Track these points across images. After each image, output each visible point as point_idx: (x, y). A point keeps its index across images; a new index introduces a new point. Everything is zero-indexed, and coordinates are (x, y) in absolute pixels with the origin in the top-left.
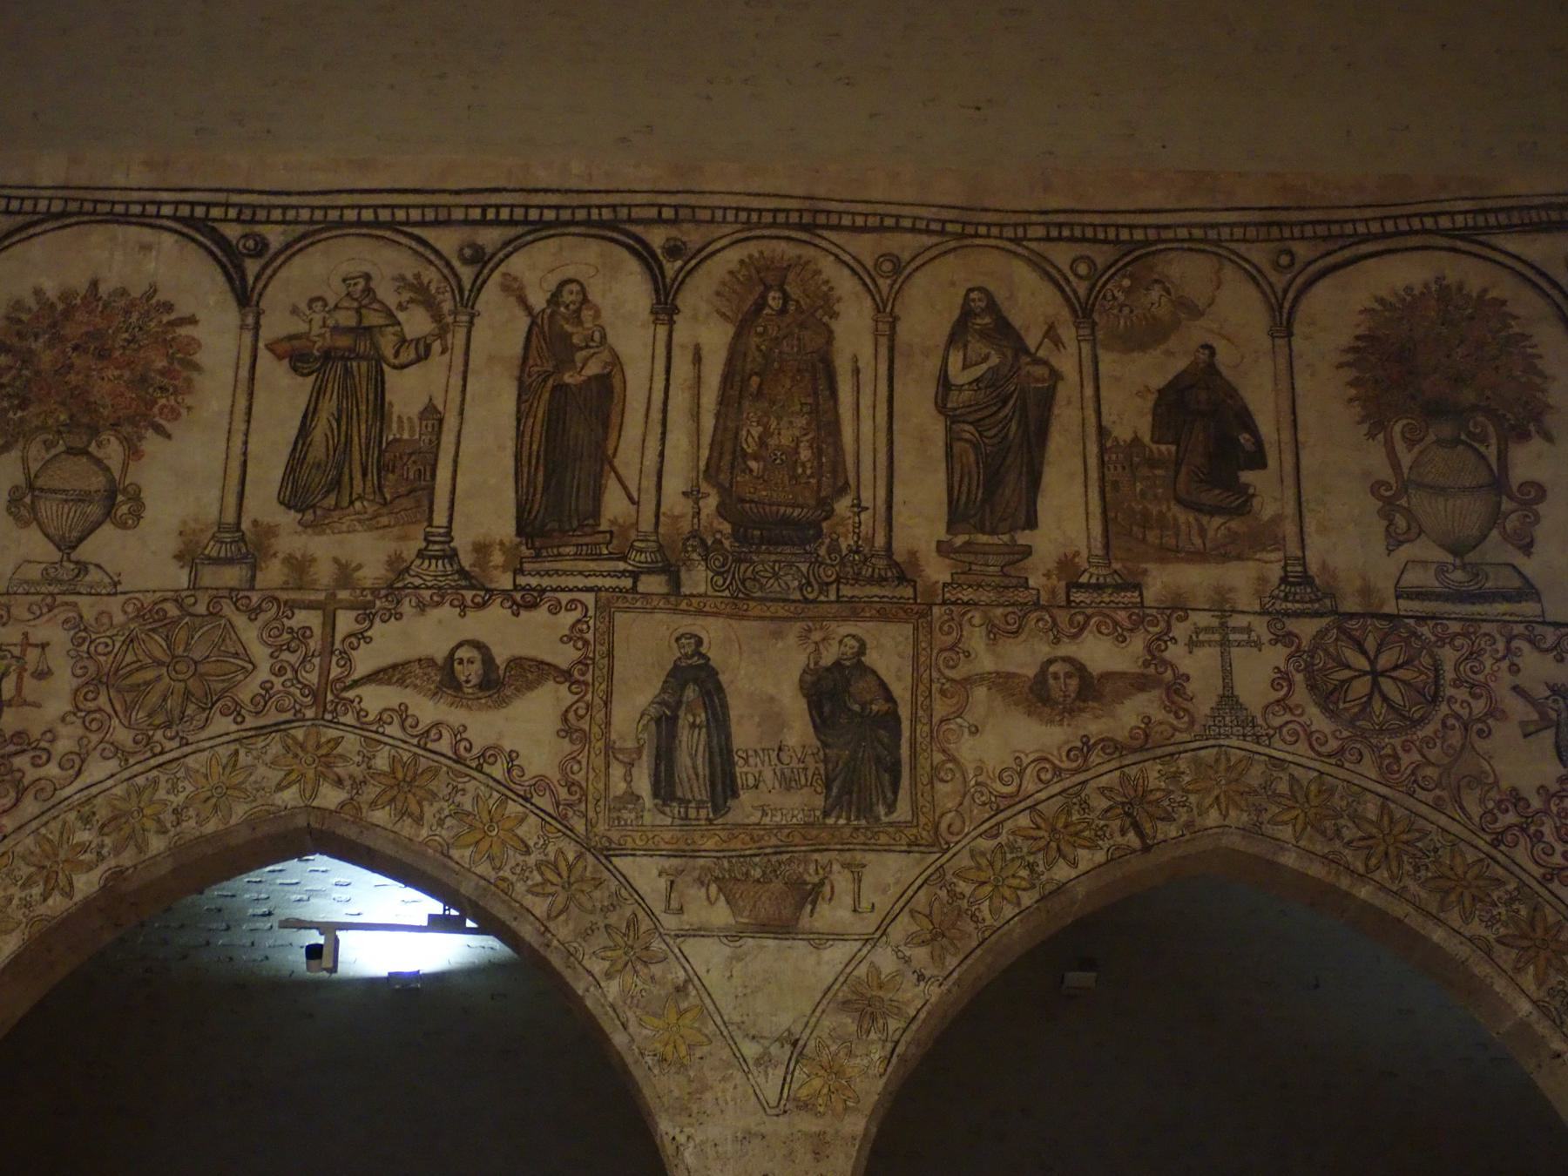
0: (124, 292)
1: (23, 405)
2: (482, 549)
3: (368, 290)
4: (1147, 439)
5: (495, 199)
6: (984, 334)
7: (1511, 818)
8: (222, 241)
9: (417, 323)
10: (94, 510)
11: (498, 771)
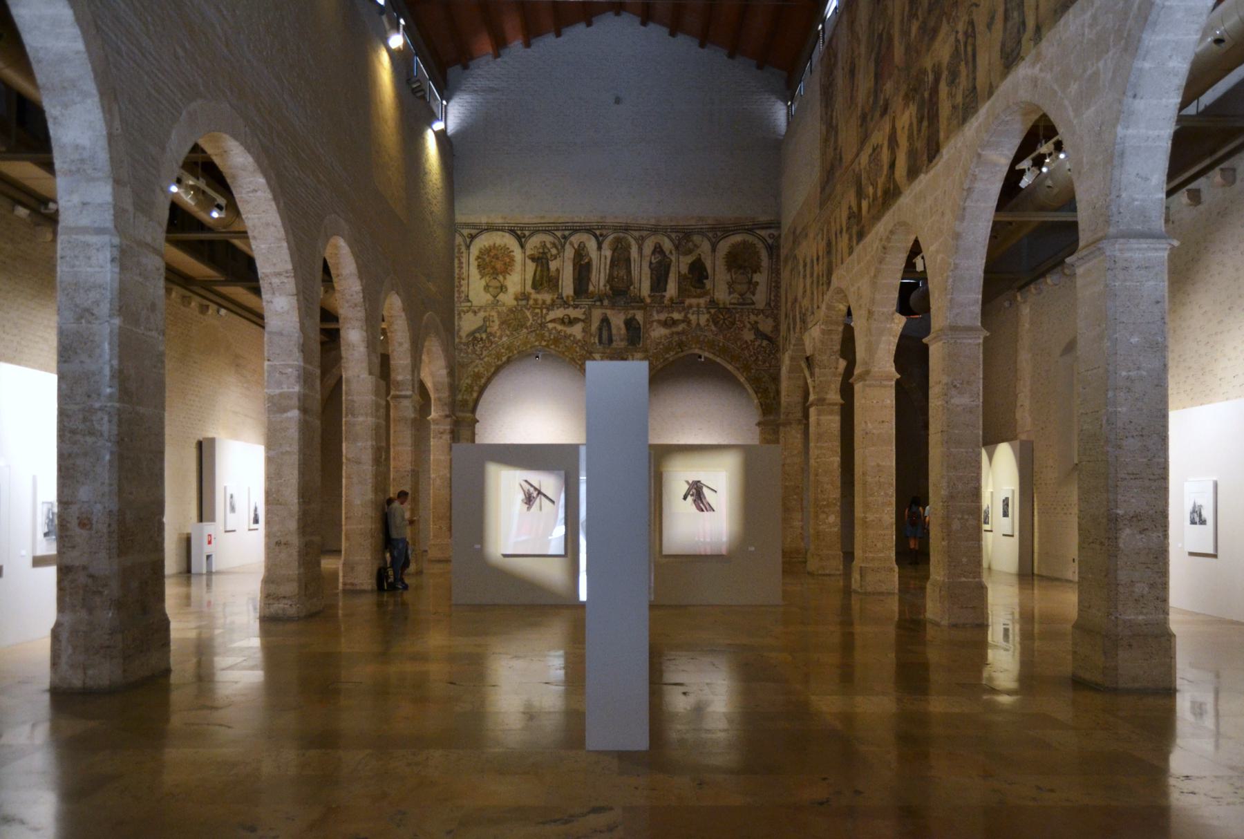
0: (500, 246)
1: (484, 269)
2: (568, 297)
3: (545, 245)
5: (567, 224)
6: (659, 252)
7: (745, 346)
8: (517, 234)
9: (554, 251)
10: (499, 290)
11: (572, 338)
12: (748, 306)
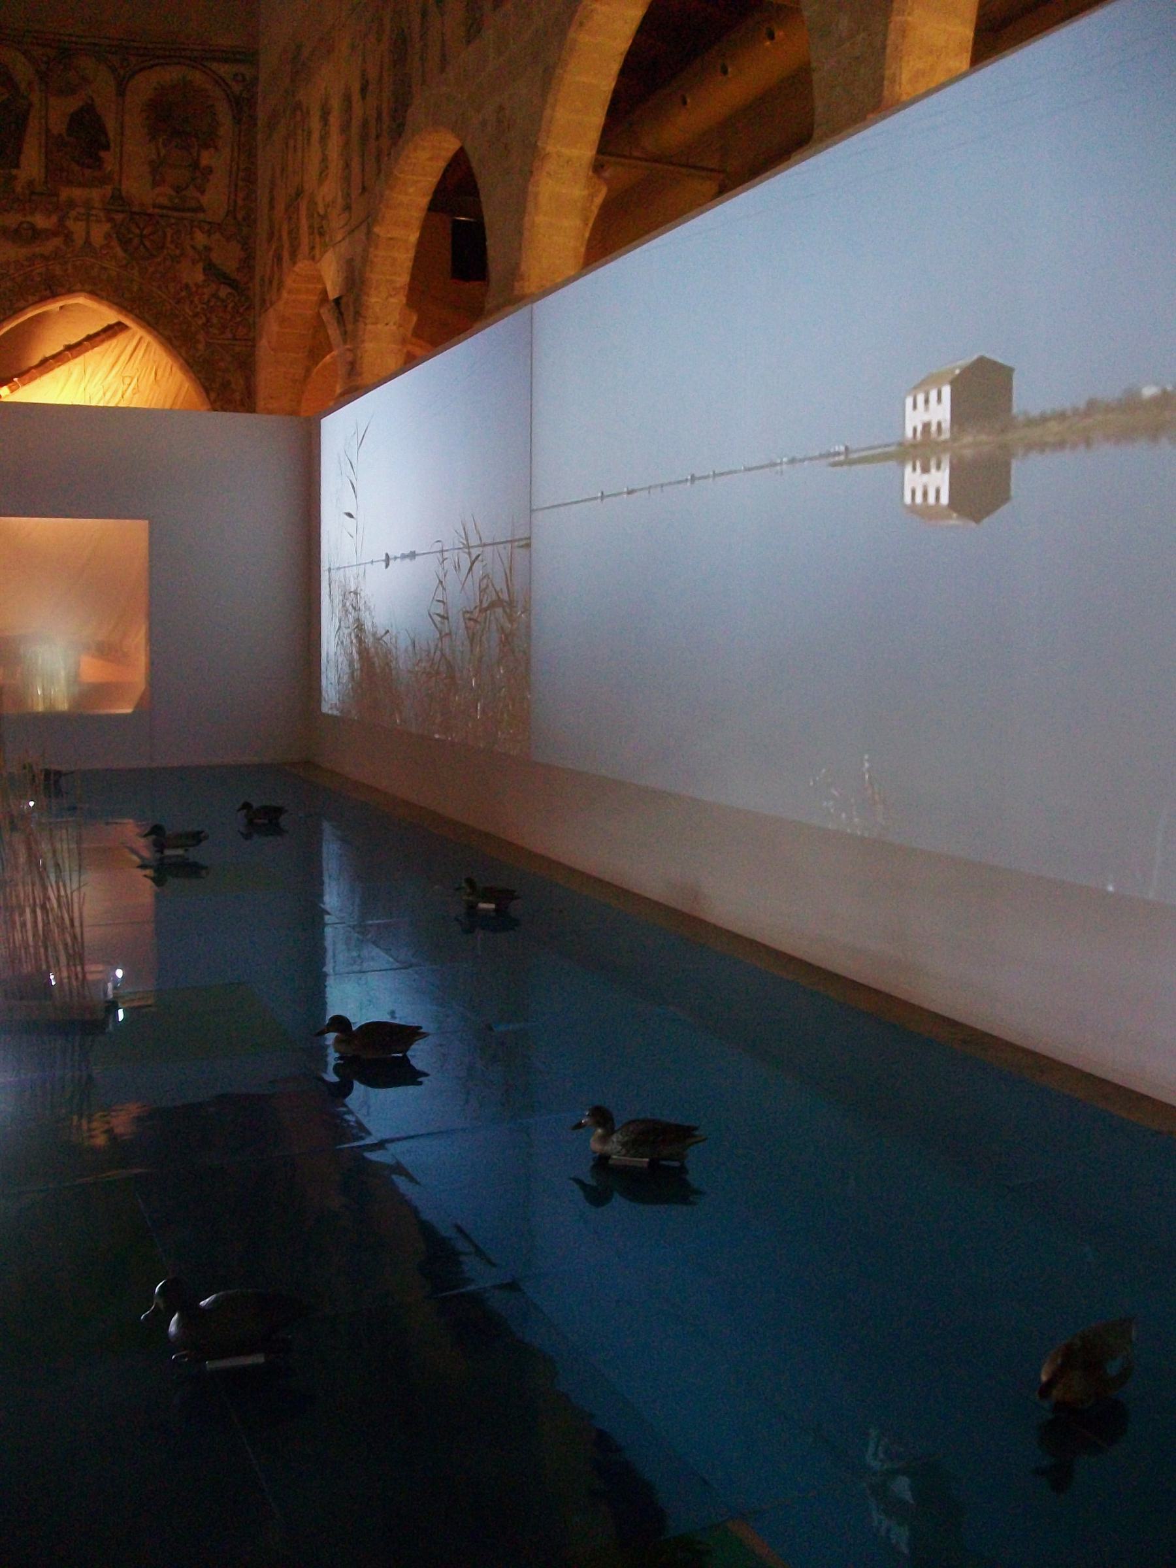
4: (65, 135)
7: (183, 294)
12: (188, 215)
